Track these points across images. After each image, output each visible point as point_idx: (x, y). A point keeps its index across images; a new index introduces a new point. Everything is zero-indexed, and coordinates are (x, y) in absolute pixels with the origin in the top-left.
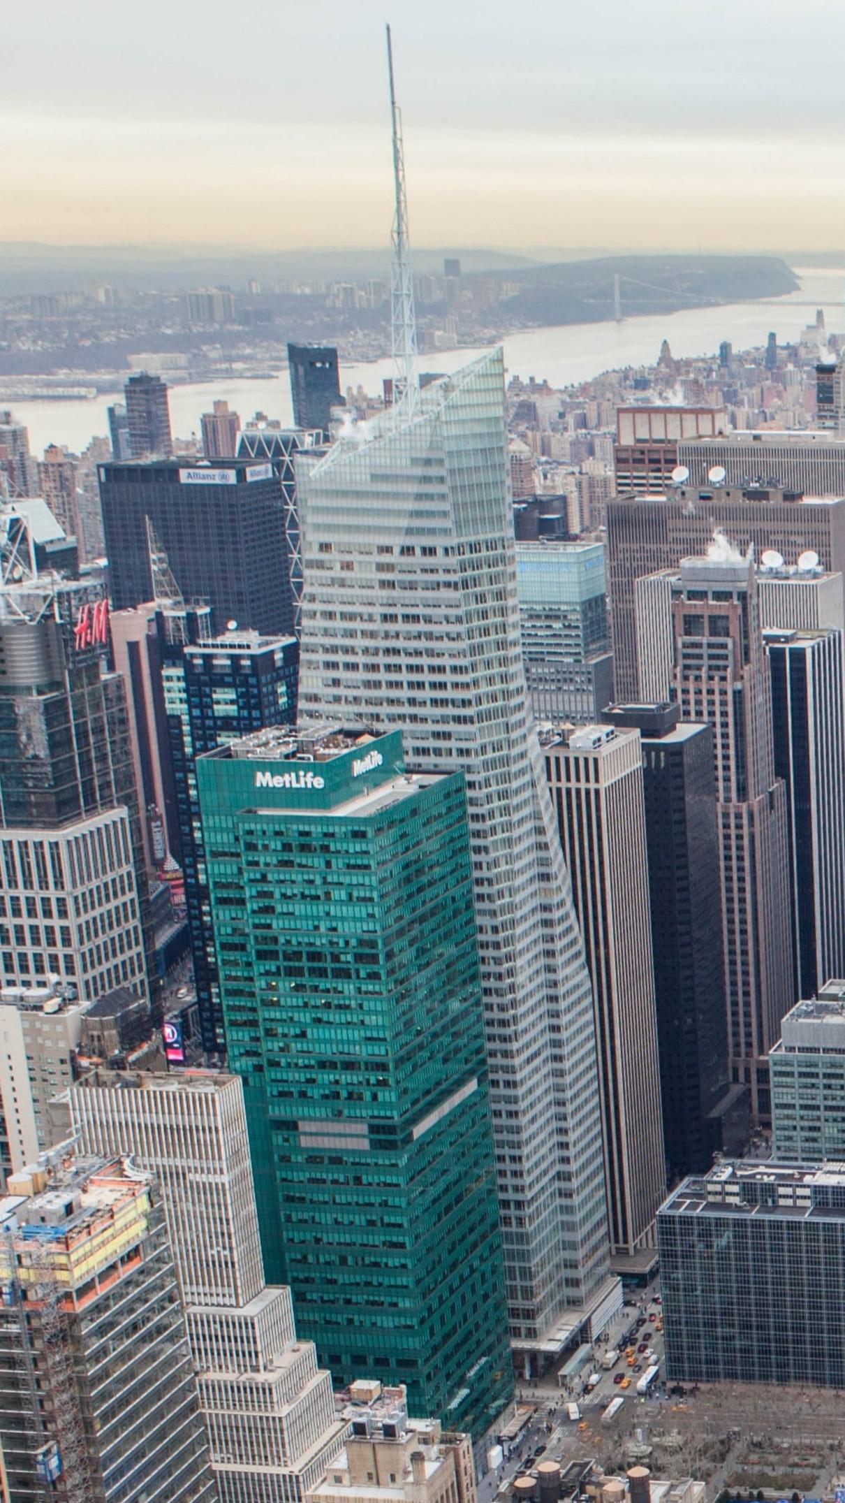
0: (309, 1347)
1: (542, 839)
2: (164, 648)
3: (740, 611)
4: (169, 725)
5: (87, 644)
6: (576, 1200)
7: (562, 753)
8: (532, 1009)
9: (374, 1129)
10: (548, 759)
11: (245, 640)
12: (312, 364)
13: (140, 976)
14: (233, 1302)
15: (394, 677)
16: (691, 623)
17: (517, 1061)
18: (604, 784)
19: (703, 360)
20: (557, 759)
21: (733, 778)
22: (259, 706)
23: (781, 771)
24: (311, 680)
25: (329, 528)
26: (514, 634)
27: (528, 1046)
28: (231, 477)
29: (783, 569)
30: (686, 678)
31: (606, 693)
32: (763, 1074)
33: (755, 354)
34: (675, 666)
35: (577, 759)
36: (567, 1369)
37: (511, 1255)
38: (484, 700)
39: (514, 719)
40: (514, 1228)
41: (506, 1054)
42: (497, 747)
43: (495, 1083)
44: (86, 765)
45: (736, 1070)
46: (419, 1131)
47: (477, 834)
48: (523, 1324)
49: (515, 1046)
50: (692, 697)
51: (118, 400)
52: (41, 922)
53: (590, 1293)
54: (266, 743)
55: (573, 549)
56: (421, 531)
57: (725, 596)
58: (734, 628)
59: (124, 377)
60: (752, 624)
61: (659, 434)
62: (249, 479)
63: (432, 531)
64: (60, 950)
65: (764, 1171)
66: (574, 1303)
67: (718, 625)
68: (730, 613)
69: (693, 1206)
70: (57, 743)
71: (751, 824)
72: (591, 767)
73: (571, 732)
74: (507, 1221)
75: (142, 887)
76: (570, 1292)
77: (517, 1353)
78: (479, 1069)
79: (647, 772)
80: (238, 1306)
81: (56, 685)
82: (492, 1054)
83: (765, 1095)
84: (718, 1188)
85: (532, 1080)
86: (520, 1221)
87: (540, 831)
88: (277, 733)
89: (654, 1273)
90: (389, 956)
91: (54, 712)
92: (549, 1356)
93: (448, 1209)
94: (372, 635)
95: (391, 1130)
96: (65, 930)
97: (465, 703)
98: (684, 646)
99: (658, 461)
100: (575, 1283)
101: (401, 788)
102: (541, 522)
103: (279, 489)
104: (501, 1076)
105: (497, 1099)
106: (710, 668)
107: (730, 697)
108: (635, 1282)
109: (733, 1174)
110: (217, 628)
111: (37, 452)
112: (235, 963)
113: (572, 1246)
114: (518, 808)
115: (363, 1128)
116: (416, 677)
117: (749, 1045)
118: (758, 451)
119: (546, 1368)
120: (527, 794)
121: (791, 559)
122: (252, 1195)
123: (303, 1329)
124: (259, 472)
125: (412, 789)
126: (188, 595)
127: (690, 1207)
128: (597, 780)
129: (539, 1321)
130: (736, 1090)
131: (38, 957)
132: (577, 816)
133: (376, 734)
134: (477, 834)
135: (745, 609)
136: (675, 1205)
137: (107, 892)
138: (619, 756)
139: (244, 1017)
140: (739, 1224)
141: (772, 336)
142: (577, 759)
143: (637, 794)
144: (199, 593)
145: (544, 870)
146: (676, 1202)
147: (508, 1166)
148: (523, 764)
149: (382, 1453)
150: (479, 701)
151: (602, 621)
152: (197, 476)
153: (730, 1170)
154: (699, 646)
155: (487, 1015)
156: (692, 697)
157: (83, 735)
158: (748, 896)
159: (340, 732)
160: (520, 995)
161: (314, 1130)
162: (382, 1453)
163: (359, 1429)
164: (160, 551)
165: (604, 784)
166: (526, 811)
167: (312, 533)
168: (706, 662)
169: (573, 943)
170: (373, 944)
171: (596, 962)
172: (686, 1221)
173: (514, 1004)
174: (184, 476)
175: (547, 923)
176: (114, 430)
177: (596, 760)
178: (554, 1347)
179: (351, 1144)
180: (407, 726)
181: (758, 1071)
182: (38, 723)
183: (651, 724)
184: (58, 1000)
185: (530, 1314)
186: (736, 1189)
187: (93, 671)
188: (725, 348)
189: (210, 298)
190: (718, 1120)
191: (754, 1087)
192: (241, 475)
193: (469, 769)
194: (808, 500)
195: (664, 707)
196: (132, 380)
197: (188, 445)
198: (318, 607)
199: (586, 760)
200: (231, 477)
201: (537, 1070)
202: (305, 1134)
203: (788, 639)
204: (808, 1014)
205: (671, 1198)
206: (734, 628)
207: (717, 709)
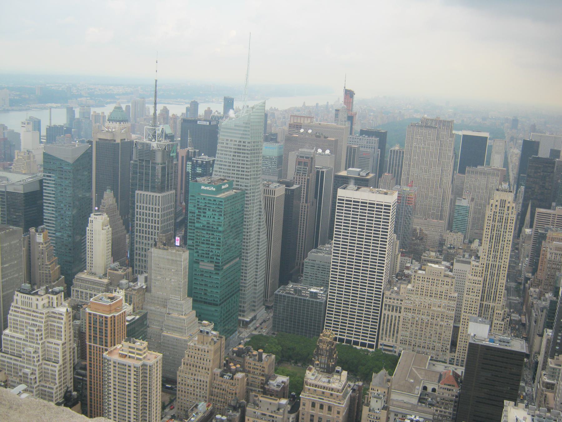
0: (194, 312)
2: (189, 158)
4: (187, 173)
6: (257, 288)
9: (215, 266)
13: (172, 227)
16: (299, 163)
17: (249, 255)
18: (275, 196)
22: (206, 172)
23: (316, 197)
24: (216, 167)
25: (224, 136)
26: (260, 162)
31: (280, 176)
32: (303, 264)
36: (250, 325)
37: (241, 298)
39: (258, 180)
40: (243, 292)
41: (247, 253)
42: (253, 185)
43: (243, 259)
44: (168, 180)
46: (225, 267)
47: (247, 204)
48: (242, 313)
49: (248, 251)
52: (154, 213)
53: (258, 309)
55: (277, 145)
56: (243, 138)
58: (309, 165)
61: (299, 121)
63: (246, 138)
65: (299, 287)
66: (254, 310)
67: (305, 164)
70: (163, 176)
74: (242, 290)
75: (176, 208)
76: (253, 308)
77: (240, 320)
78: (240, 256)
79: (286, 195)
81: (165, 163)
82: (244, 253)
83: (303, 269)
86: (244, 291)
87: (260, 205)
89: (272, 306)
92: (247, 322)
93: (229, 286)
97: (248, 176)
100: (255, 306)
101: (232, 192)
102: (271, 138)
103: (216, 126)
104: (245, 258)
105: (243, 263)
108: (268, 308)
111: (170, 115)
112: (191, 226)
113: (255, 298)
115: (213, 265)
116: (238, 169)
119: (246, 324)
122: (187, 277)
127: (283, 292)
129: (245, 314)
132: (269, 203)
134: (247, 204)
138: (280, 191)
139: (192, 238)
143: (283, 199)
146: (279, 291)
147: (243, 278)
148: (259, 190)
149: (205, 338)
150: (251, 175)
151: (281, 161)
155: (243, 244)
157: (168, 174)
160: (251, 240)
162: (205, 338)
163: (201, 331)
165: (275, 196)
167: (221, 137)
168: (302, 172)
171: (269, 235)
172: (281, 295)
173: (250, 242)
178: (248, 320)
179: (210, 268)
182: (160, 170)
183: (288, 184)
185: (244, 311)
187: (172, 161)
193: (247, 190)
195: (291, 180)
197: (200, 116)
203: (321, 169)
205: (278, 290)
206: (309, 165)
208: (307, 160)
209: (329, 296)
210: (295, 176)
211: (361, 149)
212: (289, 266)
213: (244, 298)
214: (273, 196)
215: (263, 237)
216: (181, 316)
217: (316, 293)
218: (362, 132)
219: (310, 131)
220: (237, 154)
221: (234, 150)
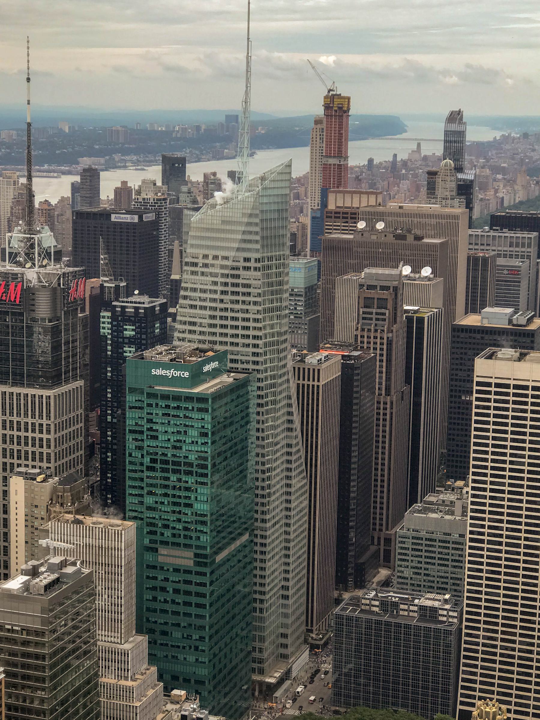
1: (290, 410)
3: (393, 296)
5: (75, 298)
7: (302, 366)
8: (278, 499)
9: (196, 555)
10: (294, 368)
11: (140, 300)
12: (173, 165)
14: (119, 641)
15: (224, 322)
16: (368, 303)
18: (322, 383)
19: (359, 167)
20: (299, 368)
21: (384, 383)
23: (408, 381)
27: (274, 517)
28: (136, 219)
29: (412, 275)
30: (363, 330)
32: (388, 541)
33: (384, 164)
34: (358, 323)
35: (309, 369)
38: (268, 336)
41: (264, 521)
43: (256, 536)
45: (373, 538)
49: (268, 517)
50: (365, 340)
51: (78, 179)
54: (158, 353)
57: (387, 288)
58: (390, 305)
59: (80, 168)
60: (399, 303)
62: (144, 220)
64: (45, 450)
67: (382, 303)
68: (389, 297)
69: (354, 611)
71: (392, 408)
72: (316, 373)
73: (306, 355)
80: (121, 644)
84: (368, 602)
85: (274, 535)
88: (166, 348)
90: (214, 465)
91: (55, 332)
94: (214, 300)
95: (205, 556)
96: (48, 440)
98: (364, 313)
99: (347, 218)
104: (258, 532)
106: (376, 325)
107: (385, 341)
109: (376, 595)
110: (129, 294)
114: (280, 393)
115: (191, 555)
117: (381, 525)
118: (401, 213)
120: (285, 386)
121: (416, 269)
123: (152, 658)
124: (149, 217)
125: (231, 380)
126: (116, 277)
128: (318, 381)
130: (373, 548)
131: (33, 453)
133: (215, 352)
135: (396, 295)
136: (344, 609)
137: (69, 423)
140: (378, 622)
141: (395, 156)
142: (309, 369)
144: (121, 275)
145: (290, 426)
148: (285, 370)
152: (120, 218)
153: (374, 593)
154: (371, 313)
156: (365, 340)
158: (387, 446)
159: (197, 349)
161: (166, 553)
164: (105, 254)
165: (322, 383)
166: (284, 395)
169: (301, 465)
170: (206, 459)
174: (113, 218)
175: (289, 454)
176: (73, 194)
177: (319, 370)
180: (229, 348)
181: (385, 539)
184: (43, 476)
186: (377, 603)
188: (371, 161)
189: (118, 131)
190: (364, 563)
191: (382, 547)
192: (141, 218)
194: (426, 240)
196: (85, 170)
198: (189, 285)
199: (314, 370)
200: (136, 219)
201: (277, 530)
202: (161, 555)
203: (416, 312)
204: (419, 512)
206: (390, 305)
207: (378, 346)
208: (385, 294)
209: (465, 616)
210: (359, 333)
211: (501, 261)
212: (354, 545)
213: (262, 629)
214: (316, 383)
215: (298, 482)
216: (123, 682)
217: (434, 610)
218: (498, 222)
219: (380, 226)
220: (230, 289)
221: (223, 280)
